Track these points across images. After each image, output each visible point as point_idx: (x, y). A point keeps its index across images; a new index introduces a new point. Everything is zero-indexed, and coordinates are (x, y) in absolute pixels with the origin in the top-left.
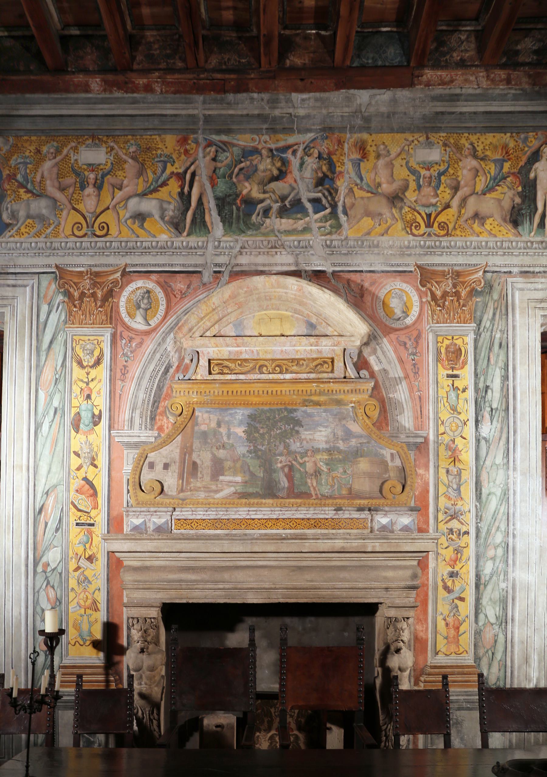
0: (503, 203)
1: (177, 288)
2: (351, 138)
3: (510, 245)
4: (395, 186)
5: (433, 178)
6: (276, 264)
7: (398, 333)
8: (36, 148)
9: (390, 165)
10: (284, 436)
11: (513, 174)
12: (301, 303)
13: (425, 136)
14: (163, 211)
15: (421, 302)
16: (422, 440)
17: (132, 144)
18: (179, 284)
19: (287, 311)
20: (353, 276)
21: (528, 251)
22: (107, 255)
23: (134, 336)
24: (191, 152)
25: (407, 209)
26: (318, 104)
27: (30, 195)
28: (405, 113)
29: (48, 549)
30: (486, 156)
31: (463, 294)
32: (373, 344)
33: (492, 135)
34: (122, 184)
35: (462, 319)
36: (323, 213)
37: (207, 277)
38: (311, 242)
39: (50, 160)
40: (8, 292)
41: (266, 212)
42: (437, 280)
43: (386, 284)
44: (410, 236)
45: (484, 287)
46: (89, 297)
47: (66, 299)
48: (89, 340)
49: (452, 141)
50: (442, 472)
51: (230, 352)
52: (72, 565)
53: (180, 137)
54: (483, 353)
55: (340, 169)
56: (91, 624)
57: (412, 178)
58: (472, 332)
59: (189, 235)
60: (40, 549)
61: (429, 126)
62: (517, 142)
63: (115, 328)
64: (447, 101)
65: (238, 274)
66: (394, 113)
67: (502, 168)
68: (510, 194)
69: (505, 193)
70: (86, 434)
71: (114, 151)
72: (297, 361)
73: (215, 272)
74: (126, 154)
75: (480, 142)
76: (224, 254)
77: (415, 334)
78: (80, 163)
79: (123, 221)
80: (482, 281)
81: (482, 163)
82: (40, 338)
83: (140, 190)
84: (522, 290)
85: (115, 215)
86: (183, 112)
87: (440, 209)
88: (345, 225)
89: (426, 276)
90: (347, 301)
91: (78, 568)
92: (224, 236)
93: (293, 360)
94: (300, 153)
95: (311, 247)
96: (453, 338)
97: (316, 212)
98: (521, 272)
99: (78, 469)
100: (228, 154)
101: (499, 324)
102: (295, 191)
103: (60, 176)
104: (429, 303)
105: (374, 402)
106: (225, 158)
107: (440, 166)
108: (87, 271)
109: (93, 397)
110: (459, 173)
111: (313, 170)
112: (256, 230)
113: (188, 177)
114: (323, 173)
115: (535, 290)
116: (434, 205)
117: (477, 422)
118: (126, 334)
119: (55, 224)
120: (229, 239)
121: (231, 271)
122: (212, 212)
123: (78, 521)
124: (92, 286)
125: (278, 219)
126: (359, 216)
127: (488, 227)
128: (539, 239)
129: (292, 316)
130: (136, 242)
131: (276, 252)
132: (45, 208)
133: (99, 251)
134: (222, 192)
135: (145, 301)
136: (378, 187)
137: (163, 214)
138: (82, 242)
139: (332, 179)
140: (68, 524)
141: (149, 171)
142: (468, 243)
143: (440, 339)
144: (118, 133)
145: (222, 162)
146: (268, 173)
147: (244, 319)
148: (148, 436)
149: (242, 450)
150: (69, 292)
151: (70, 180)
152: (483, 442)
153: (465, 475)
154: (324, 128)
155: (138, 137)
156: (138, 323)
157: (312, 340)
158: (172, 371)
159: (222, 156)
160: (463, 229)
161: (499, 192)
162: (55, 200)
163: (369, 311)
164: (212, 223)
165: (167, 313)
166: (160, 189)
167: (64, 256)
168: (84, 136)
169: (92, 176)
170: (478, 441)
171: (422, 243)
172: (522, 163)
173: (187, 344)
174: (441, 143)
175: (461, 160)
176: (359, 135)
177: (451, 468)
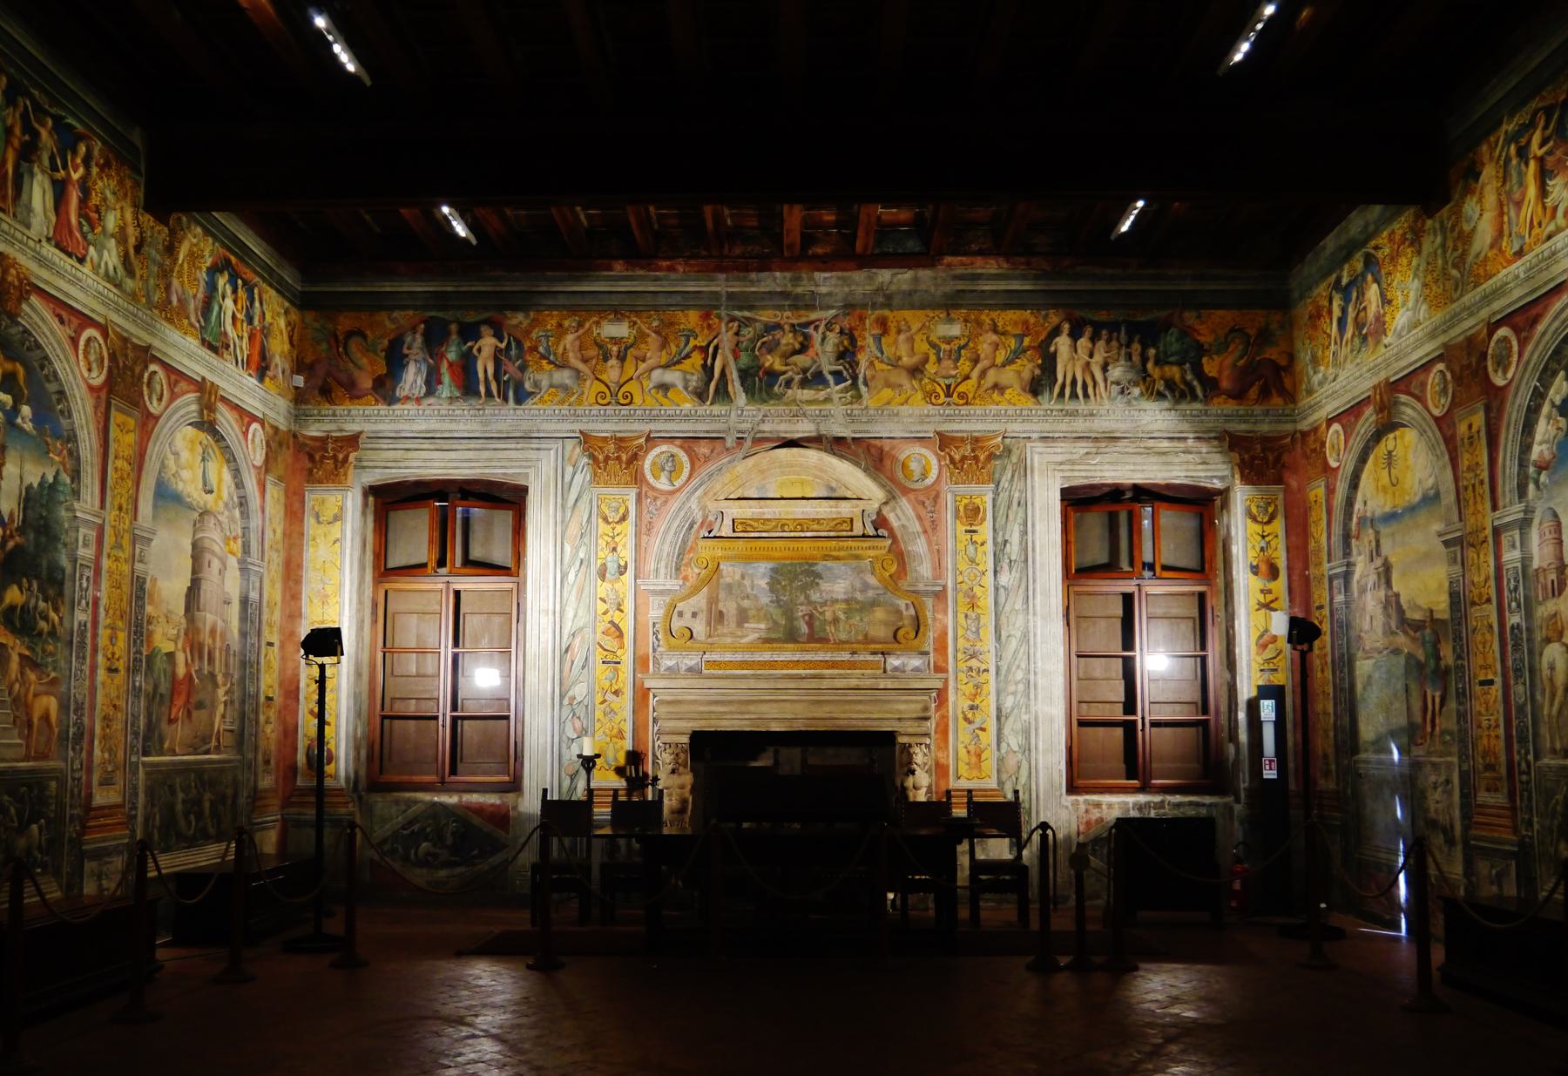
12: (821, 470)
14: (686, 382)
15: (940, 467)
18: (703, 449)
31: (982, 457)
32: (892, 503)
37: (730, 442)
41: (788, 383)
50: (961, 617)
72: (818, 521)
83: (663, 361)
89: (945, 441)
97: (837, 384)
105: (891, 556)
106: (748, 333)
113: (711, 350)
117: (995, 572)
139: (854, 354)
151: (593, 352)
152: (1002, 591)
153: (983, 620)
159: (744, 331)
160: (982, 398)
162: (578, 371)
169: (615, 349)
170: (997, 589)
173: (713, 507)
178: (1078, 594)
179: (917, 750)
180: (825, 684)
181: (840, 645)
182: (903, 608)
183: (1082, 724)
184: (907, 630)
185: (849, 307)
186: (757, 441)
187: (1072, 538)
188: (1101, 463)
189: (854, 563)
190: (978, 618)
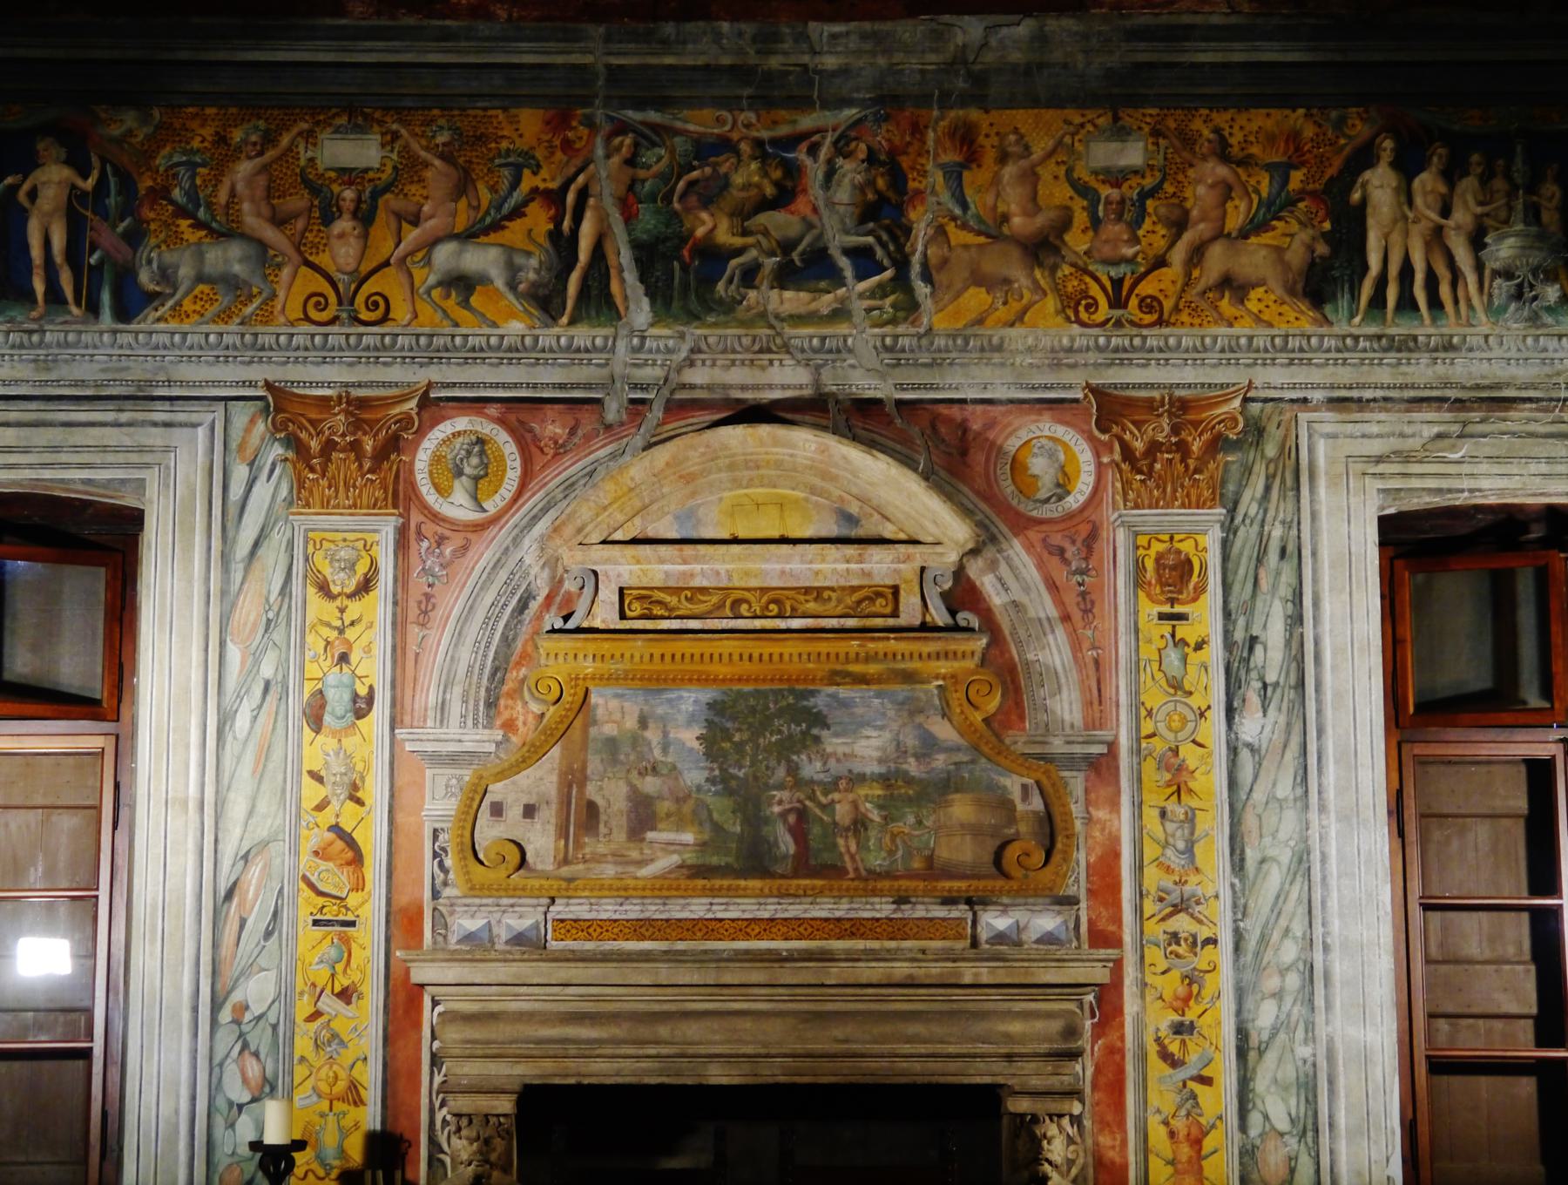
0: (1288, 256)
2: (942, 118)
3: (1304, 342)
4: (1040, 221)
5: (1128, 203)
6: (770, 387)
7: (1044, 528)
8: (217, 133)
9: (1031, 177)
10: (787, 748)
11: (1313, 194)
13: (1110, 114)
14: (513, 271)
15: (1100, 466)
16: (1103, 749)
17: (441, 128)
18: (552, 427)
20: (943, 410)
21: (1346, 355)
22: (385, 364)
23: (447, 533)
24: (577, 146)
25: (1067, 270)
26: (868, 46)
27: (203, 233)
28: (1065, 66)
29: (246, 973)
30: (1250, 156)
31: (1196, 447)
32: (989, 552)
33: (1264, 111)
34: (420, 210)
35: (1194, 499)
36: (877, 278)
37: (613, 411)
38: (850, 341)
39: (250, 158)
40: (155, 437)
41: (749, 276)
47: (290, 455)
49: (1173, 125)
50: (1151, 817)
51: (667, 574)
52: (304, 1007)
54: (1243, 569)
56: (344, 1133)
57: (1079, 205)
60: (228, 974)
62: (1320, 126)
63: (406, 516)
66: (1041, 66)
67: (1286, 180)
68: (1304, 236)
69: (1292, 236)
70: (338, 735)
72: (818, 593)
73: (633, 401)
74: (427, 149)
75: (1236, 128)
76: (654, 364)
77: (1084, 530)
78: (321, 167)
80: (1241, 419)
81: (1240, 170)
82: (231, 534)
83: (461, 224)
84: (1334, 436)
85: (405, 280)
86: (560, 59)
87: (1142, 269)
88: (927, 304)
89: (1109, 410)
91: (316, 1015)
92: (652, 325)
93: (807, 590)
95: (850, 351)
96: (1172, 538)
97: (860, 277)
98: (1331, 400)
99: (320, 807)
100: (663, 152)
101: (1280, 508)
102: (815, 232)
103: (272, 192)
104: (1117, 465)
106: (657, 159)
107: (1143, 177)
108: (340, 397)
109: (354, 658)
110: (1188, 193)
111: (854, 187)
112: (725, 313)
113: (571, 198)
114: (877, 192)
115: (1363, 436)
116: (1131, 261)
117: (1230, 712)
118: (429, 528)
119: (264, 295)
120: (666, 332)
121: (668, 401)
122: (626, 275)
123: (318, 917)
124: (351, 428)
126: (958, 285)
127: (1252, 305)
128: (1372, 330)
129: (806, 500)
130: (453, 336)
132: (240, 261)
134: (647, 231)
135: (475, 461)
136: (1001, 223)
138: (327, 335)
139: (900, 209)
140: (295, 924)
141: (481, 186)
142: (1208, 341)
143: (1142, 540)
144: (408, 103)
145: (649, 167)
146: (754, 192)
147: (699, 505)
148: (482, 739)
149: (695, 776)
150: (298, 441)
151: (297, 201)
152: (1245, 754)
153: (1203, 823)
156: (457, 506)
157: (850, 550)
158: (534, 606)
161: (1279, 231)
162: (262, 245)
163: (980, 483)
164: (626, 298)
165: (515, 499)
169: (349, 194)
170: (1233, 751)
171: (1102, 340)
172: (1331, 172)
174: (1147, 129)
175: (1191, 165)
176: (961, 112)
177: (1171, 806)
178: (1422, 762)
179: (1052, 1130)
180: (835, 973)
181: (869, 882)
182: (1016, 795)
183: (1440, 1066)
184: (1025, 845)
185: (888, 101)
186: (678, 408)
187: (1407, 632)
188: (1473, 459)
189: (901, 690)
190: (1190, 819)
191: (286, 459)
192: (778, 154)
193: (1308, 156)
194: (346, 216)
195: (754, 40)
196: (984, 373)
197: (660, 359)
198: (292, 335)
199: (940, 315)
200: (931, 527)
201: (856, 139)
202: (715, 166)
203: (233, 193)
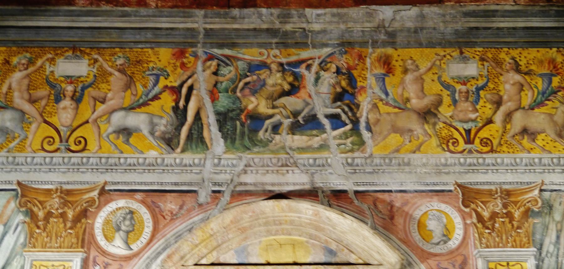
0: (556, 118)
1: (167, 208)
2: (374, 52)
4: (426, 102)
5: (471, 92)
6: (287, 184)
7: (437, 258)
8: (5, 59)
9: (420, 80)
12: (318, 228)
13: (458, 51)
15: (465, 224)
17: (120, 57)
18: (170, 205)
19: (300, 236)
22: (82, 172)
23: (110, 262)
24: (189, 65)
25: (441, 125)
26: (335, 19)
30: (531, 70)
34: (106, 97)
35: (518, 242)
37: (203, 196)
38: (329, 160)
39: (20, 71)
41: (276, 128)
42: (483, 200)
43: (421, 205)
44: (447, 153)
45: (542, 207)
46: (56, 217)
47: (28, 219)
48: (53, 266)
53: (176, 50)
55: (361, 84)
57: (445, 93)
58: (533, 258)
59: (183, 151)
61: (463, 42)
63: (88, 253)
64: (482, 17)
65: (241, 195)
66: (422, 29)
67: (550, 82)
69: (556, 108)
71: (99, 64)
73: (214, 192)
74: (112, 67)
77: (460, 259)
78: (57, 75)
79: (104, 135)
80: (539, 200)
81: (526, 77)
83: (127, 103)
85: (95, 130)
86: (181, 26)
87: (480, 125)
89: (469, 196)
90: (374, 228)
92: (225, 153)
94: (315, 68)
95: (329, 165)
96: (508, 264)
97: (334, 128)
100: (232, 68)
102: (310, 107)
104: (475, 225)
106: (228, 72)
107: (477, 80)
108: (57, 189)
110: (501, 88)
111: (330, 85)
112: (264, 147)
113: (184, 90)
114: (342, 88)
118: (101, 259)
119: (22, 137)
120: (232, 156)
121: (233, 191)
122: (212, 128)
124: (62, 206)
125: (290, 136)
126: (385, 133)
127: (540, 142)
129: (307, 242)
130: (119, 158)
131: (287, 171)
133: (73, 167)
134: (224, 107)
135: (127, 223)
136: (406, 102)
137: (153, 129)
138: (52, 158)
139: (353, 95)
144: (103, 45)
145: (224, 76)
146: (278, 88)
147: (248, 245)
150: (32, 211)
151: (43, 92)
154: (343, 43)
155: (128, 50)
159: (224, 70)
160: (510, 145)
161: (549, 106)
162: (23, 113)
163: (402, 235)
164: (211, 139)
166: (150, 102)
167: (28, 172)
168: (63, 47)
174: (477, 58)
175: (501, 75)
176: (383, 50)
191: (25, 222)
192: (290, 69)
193: (560, 70)
194: (68, 99)
195: (278, 17)
196: (401, 177)
197: (228, 170)
198: (34, 157)
199: (376, 147)
200: (376, 256)
201: (330, 62)
202: (258, 75)
203: (10, 88)
